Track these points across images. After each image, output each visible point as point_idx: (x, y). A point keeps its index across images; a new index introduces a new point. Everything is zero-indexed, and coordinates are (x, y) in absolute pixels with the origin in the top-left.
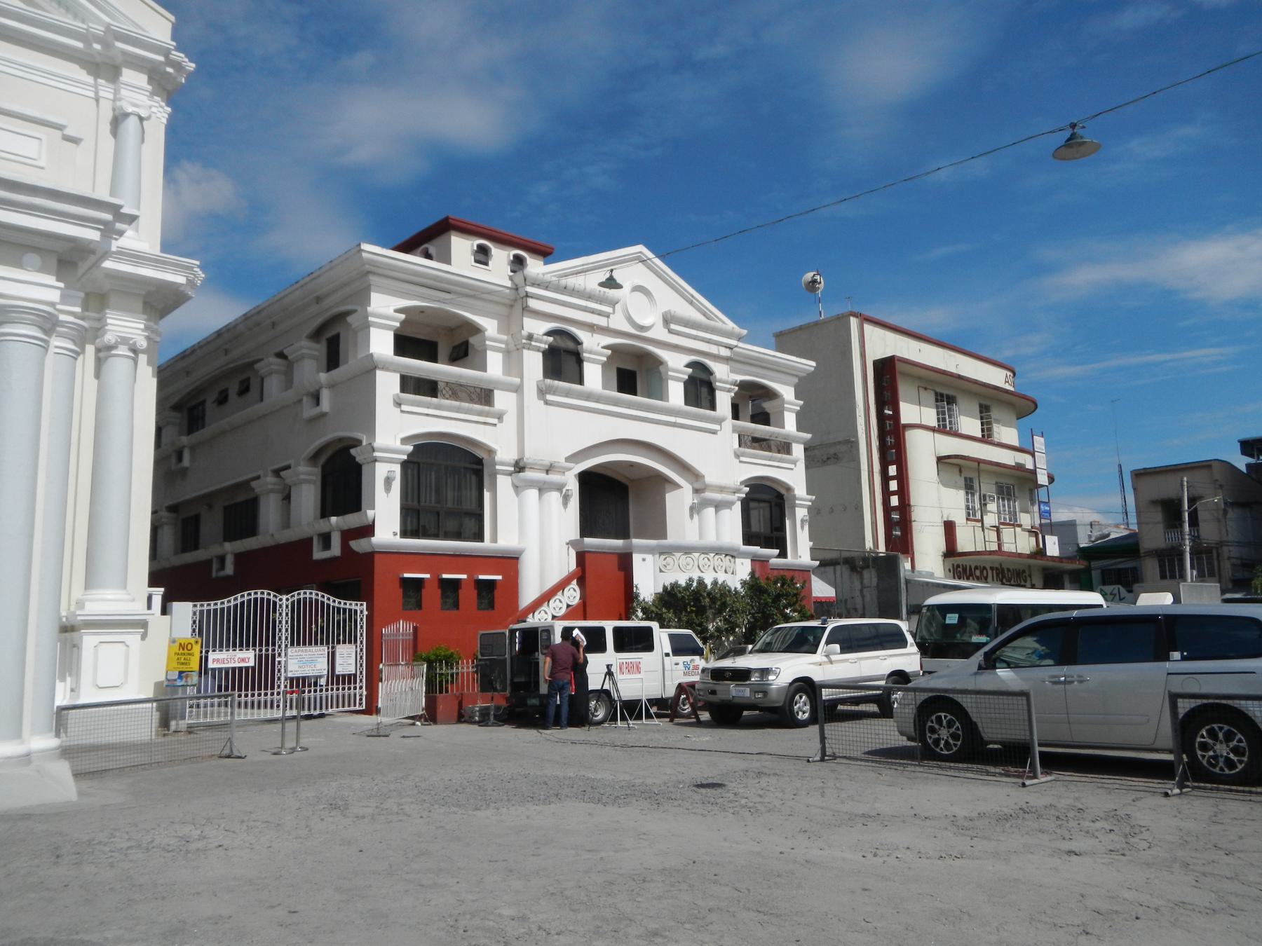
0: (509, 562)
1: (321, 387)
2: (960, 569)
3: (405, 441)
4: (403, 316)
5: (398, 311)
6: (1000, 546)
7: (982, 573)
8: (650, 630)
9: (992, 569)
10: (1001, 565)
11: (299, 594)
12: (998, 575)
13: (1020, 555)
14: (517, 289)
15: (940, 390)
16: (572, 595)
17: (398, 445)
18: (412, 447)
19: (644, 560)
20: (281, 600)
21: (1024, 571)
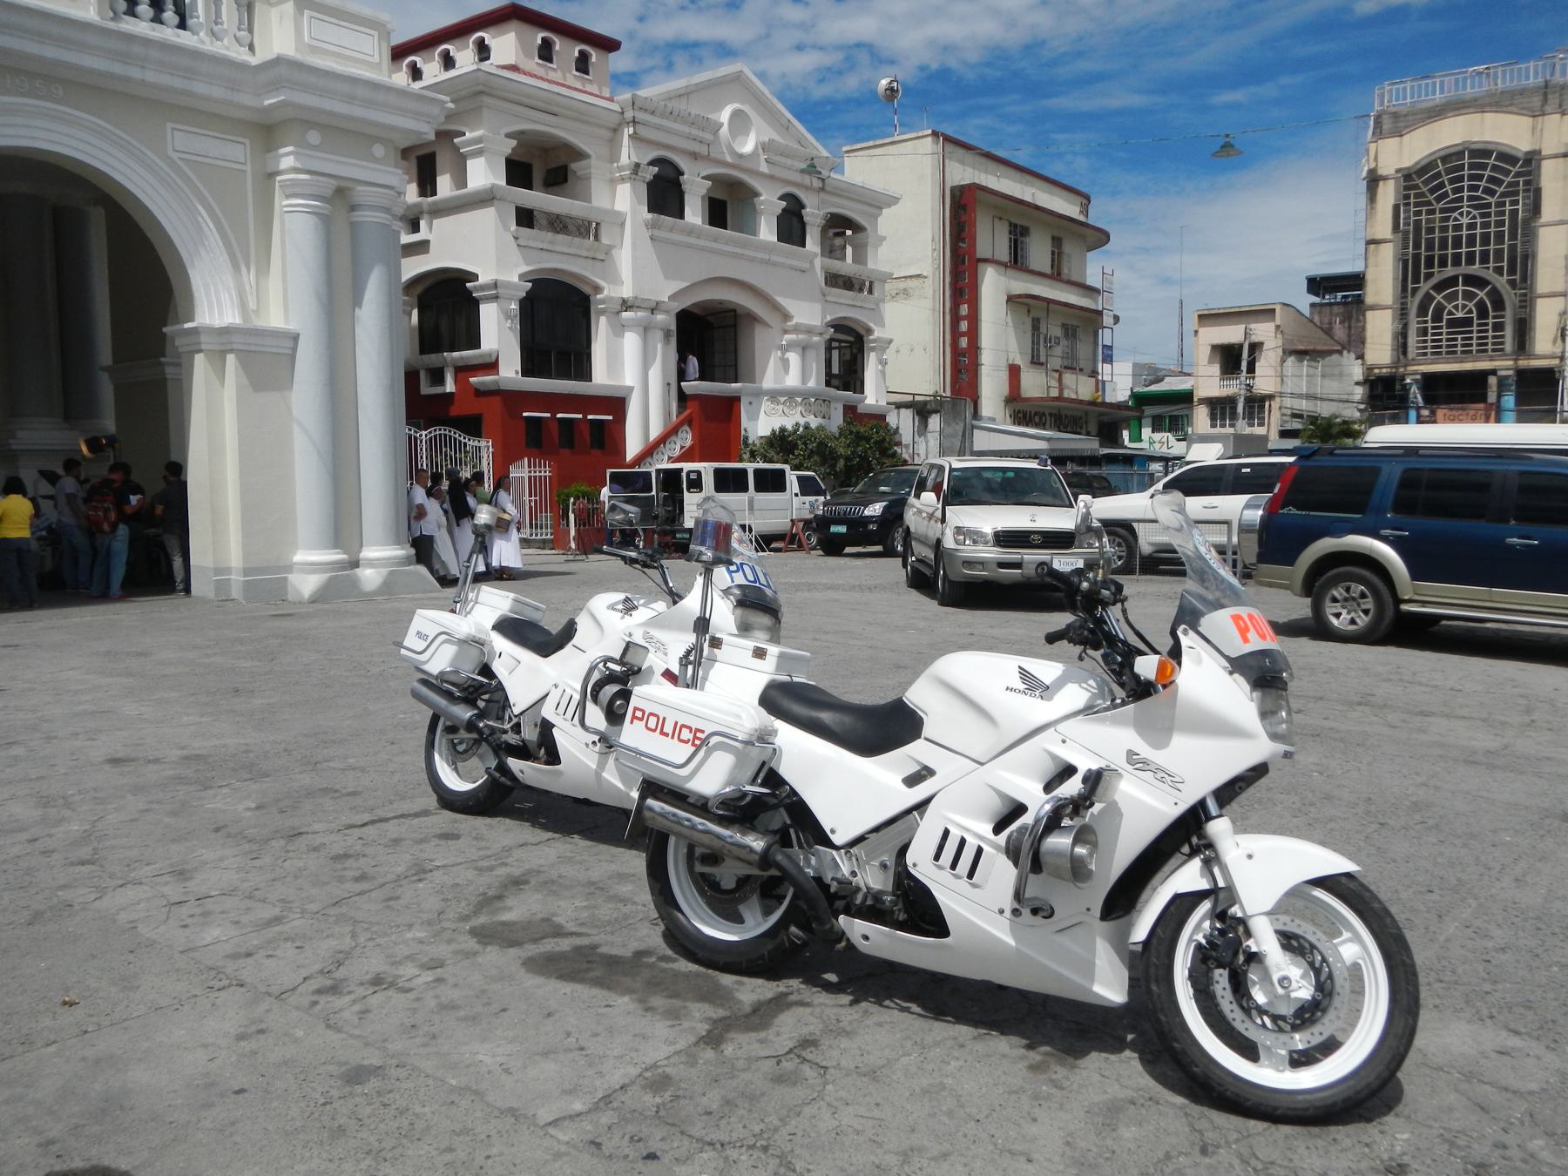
0: (616, 405)
1: (422, 213)
2: (1020, 415)
3: (521, 277)
4: (514, 143)
5: (508, 136)
6: (1061, 391)
7: (1041, 419)
8: (782, 472)
9: (1051, 415)
10: (1059, 411)
11: (435, 430)
12: (1055, 422)
13: (1081, 402)
14: (623, 113)
15: (1014, 220)
16: (686, 438)
17: (516, 279)
18: (530, 284)
19: (750, 403)
20: (421, 436)
21: (1081, 418)
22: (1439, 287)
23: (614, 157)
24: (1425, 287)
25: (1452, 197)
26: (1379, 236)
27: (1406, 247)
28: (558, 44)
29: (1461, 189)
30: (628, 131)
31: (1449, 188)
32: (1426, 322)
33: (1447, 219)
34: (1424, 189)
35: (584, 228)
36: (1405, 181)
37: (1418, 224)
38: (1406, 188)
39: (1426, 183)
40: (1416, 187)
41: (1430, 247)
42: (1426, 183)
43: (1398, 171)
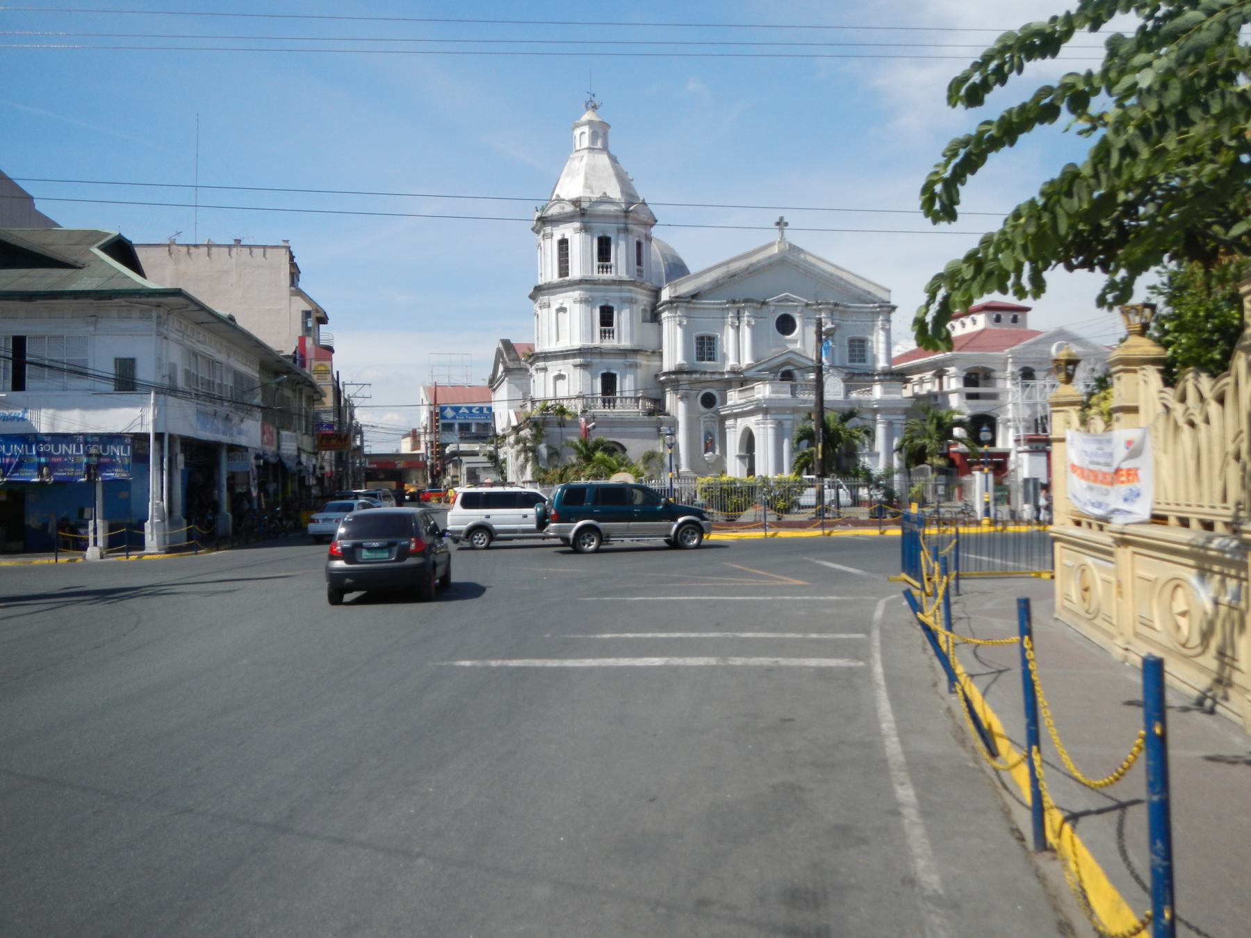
23: (1005, 370)
28: (1003, 315)
30: (1010, 360)
35: (994, 396)
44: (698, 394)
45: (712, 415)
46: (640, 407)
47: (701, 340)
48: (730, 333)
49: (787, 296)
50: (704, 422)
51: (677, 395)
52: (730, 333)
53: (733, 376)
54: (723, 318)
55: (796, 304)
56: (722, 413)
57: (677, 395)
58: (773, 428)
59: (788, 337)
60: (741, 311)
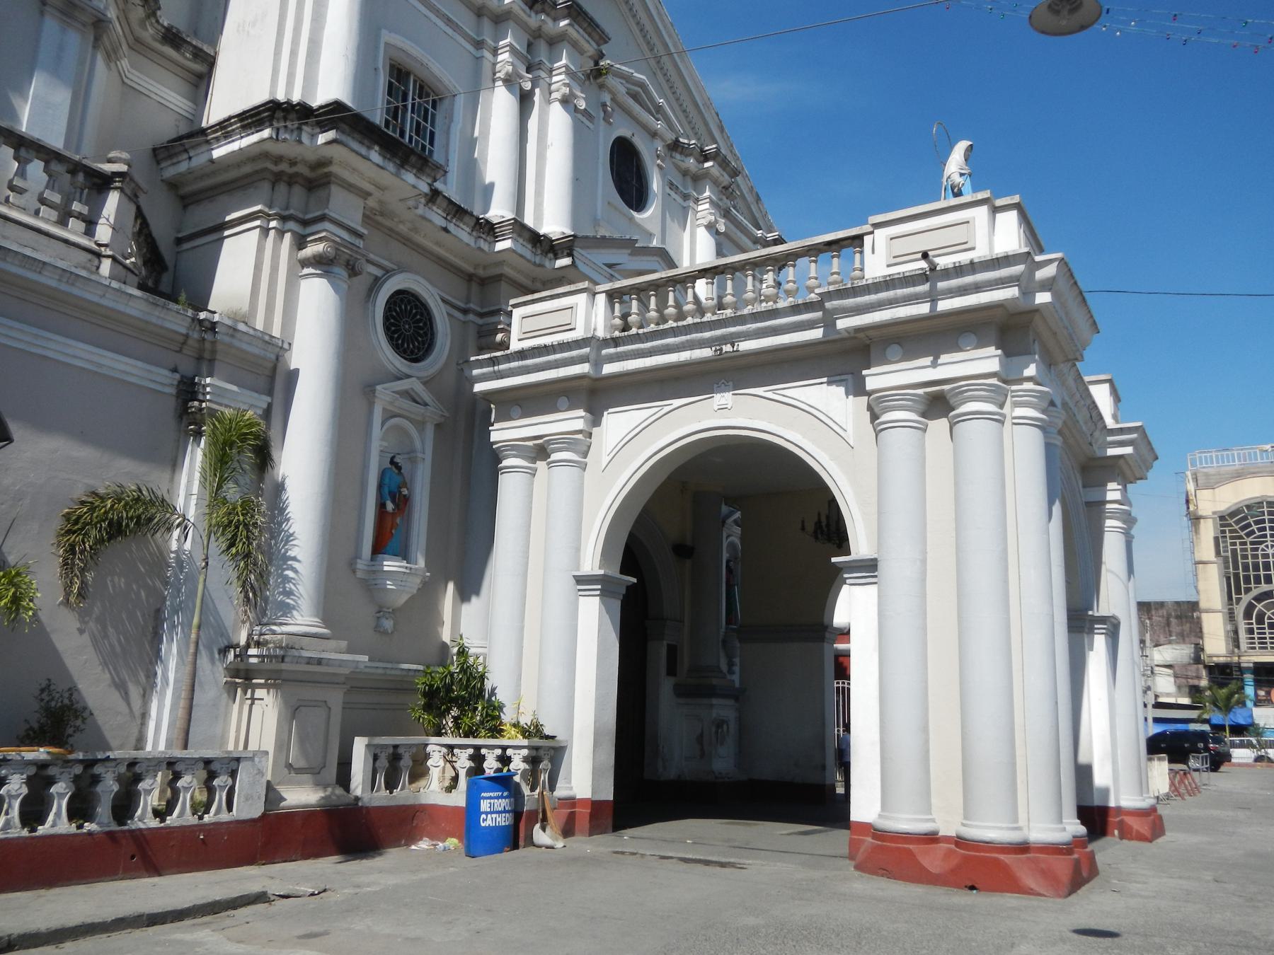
22: (1259, 598)
24: (1246, 598)
25: (1258, 534)
26: (1205, 559)
27: (1227, 567)
29: (1264, 529)
31: (1255, 527)
32: (1252, 624)
33: (1257, 549)
34: (1237, 527)
36: (1220, 520)
37: (1234, 552)
38: (1222, 526)
39: (1237, 522)
40: (1230, 525)
41: (1246, 568)
42: (1237, 522)
43: (1214, 513)
44: (376, 283)
45: (419, 388)
46: (103, 233)
47: (399, 75)
48: (501, 103)
49: (641, 85)
50: (389, 415)
51: (300, 243)
52: (501, 103)
53: (527, 251)
54: (479, 45)
55: (659, 125)
56: (478, 387)
57: (300, 243)
58: (1043, 427)
59: (634, 214)
60: (542, 47)
